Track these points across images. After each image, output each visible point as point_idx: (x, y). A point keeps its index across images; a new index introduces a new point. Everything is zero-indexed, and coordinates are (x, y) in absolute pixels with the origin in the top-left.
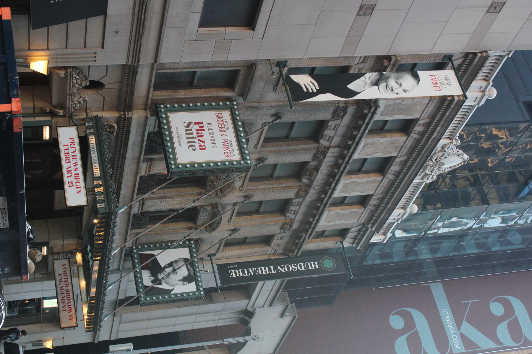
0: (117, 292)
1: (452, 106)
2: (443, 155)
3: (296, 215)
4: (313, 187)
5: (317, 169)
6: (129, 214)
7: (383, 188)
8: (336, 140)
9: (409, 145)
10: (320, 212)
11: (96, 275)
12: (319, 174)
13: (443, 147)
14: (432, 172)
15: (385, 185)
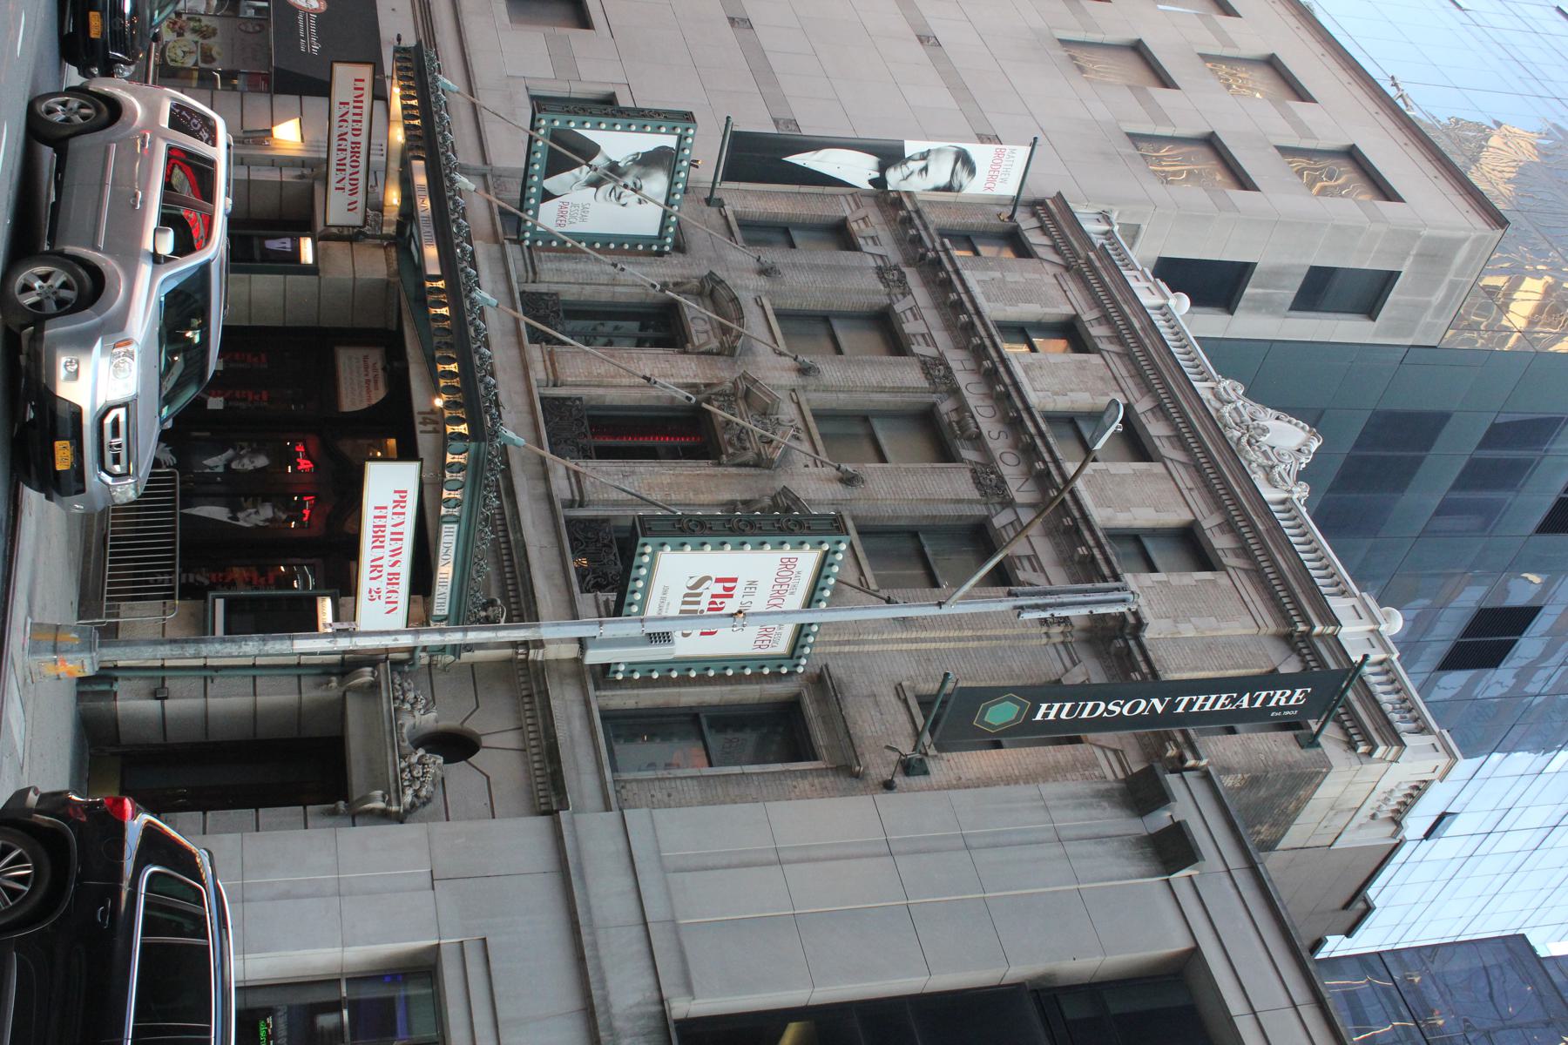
0: (641, 947)
1: (1097, 264)
2: (1236, 409)
3: (1043, 570)
4: (997, 456)
5: (962, 408)
6: (549, 497)
7: (1195, 493)
8: (941, 337)
9: (1125, 373)
10: (1077, 515)
11: (427, 203)
12: (979, 419)
13: (1217, 395)
14: (1268, 458)
15: (1190, 485)
